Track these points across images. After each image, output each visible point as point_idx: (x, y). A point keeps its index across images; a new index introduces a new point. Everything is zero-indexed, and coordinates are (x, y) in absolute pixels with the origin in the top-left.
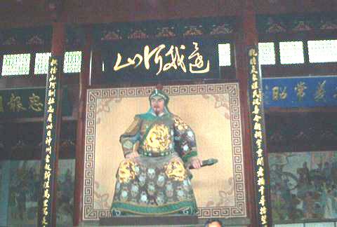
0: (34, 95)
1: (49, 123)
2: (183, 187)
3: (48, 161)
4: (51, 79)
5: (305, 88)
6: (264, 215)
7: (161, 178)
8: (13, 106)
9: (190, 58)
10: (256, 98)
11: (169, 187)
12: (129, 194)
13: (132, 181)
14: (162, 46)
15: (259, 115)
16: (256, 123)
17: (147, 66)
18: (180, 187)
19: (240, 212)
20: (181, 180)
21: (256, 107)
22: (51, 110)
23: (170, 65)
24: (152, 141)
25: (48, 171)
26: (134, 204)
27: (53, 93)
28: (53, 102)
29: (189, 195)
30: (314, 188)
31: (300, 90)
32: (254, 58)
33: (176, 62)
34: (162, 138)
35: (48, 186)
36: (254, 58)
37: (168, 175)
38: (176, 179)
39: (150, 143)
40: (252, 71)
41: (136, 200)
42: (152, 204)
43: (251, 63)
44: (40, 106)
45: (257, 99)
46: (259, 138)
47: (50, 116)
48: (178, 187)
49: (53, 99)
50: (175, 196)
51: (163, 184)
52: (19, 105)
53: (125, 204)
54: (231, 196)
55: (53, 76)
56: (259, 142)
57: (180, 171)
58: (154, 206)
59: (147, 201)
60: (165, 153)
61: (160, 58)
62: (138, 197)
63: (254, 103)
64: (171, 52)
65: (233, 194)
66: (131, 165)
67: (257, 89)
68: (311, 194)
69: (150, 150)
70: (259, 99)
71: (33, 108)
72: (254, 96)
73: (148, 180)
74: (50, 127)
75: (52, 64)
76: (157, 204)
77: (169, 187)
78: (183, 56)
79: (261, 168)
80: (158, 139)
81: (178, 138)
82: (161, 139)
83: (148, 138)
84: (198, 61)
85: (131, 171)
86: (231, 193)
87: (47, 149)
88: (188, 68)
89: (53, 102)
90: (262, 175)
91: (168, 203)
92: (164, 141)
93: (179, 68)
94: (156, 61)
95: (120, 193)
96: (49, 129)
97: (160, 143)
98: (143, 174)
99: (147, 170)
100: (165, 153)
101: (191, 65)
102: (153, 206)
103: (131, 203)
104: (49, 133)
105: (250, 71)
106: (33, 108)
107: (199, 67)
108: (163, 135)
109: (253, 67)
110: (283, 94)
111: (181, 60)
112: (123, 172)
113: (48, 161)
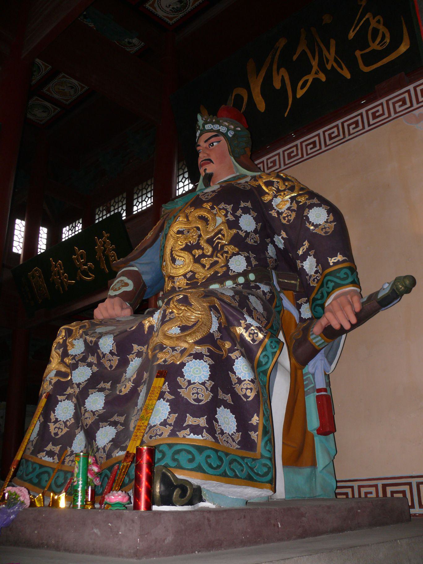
2: (174, 388)
9: (351, 35)
14: (282, 43)
17: (261, 106)
23: (310, 78)
33: (322, 66)
34: (203, 243)
41: (57, 449)
51: (130, 385)
61: (283, 72)
64: (302, 47)
78: (333, 42)
80: (188, 249)
82: (198, 246)
84: (375, 32)
88: (352, 66)
92: (209, 250)
93: (332, 74)
94: (277, 85)
97: (197, 260)
101: (358, 53)
107: (379, 48)
111: (331, 55)
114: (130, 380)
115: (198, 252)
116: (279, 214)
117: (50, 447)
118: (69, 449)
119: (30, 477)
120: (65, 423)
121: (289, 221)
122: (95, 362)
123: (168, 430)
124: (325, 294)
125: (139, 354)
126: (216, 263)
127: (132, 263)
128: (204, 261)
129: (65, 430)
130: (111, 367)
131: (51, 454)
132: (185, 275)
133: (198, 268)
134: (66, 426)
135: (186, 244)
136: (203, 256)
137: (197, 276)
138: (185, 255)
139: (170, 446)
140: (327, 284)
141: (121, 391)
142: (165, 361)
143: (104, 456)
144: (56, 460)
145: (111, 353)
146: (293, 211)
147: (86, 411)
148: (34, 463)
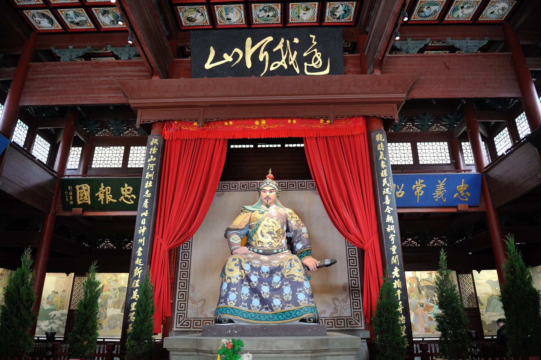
0: (126, 185)
1: (144, 210)
2: (304, 290)
3: (140, 254)
4: (149, 161)
5: (424, 186)
6: (402, 325)
7: (276, 279)
8: (101, 197)
10: (386, 186)
11: (287, 290)
12: (238, 297)
13: (242, 281)
15: (390, 205)
16: (388, 216)
18: (301, 289)
19: (357, 324)
20: (300, 280)
21: (387, 197)
22: (148, 194)
24: (263, 236)
25: (139, 266)
26: (244, 308)
27: (151, 175)
28: (150, 185)
29: (310, 300)
30: (426, 299)
31: (419, 187)
32: (382, 143)
35: (137, 285)
36: (382, 143)
37: (285, 275)
38: (296, 279)
39: (260, 238)
40: (381, 158)
41: (246, 304)
42: (267, 309)
43: (379, 149)
44: (132, 198)
45: (388, 189)
46: (392, 232)
47: (146, 201)
48: (298, 290)
49: (151, 182)
50: (295, 301)
51: (279, 285)
52: (109, 198)
53: (232, 308)
54: (346, 304)
55: (152, 156)
56: (392, 238)
57: (300, 270)
58: (269, 312)
59: (260, 306)
60: (278, 250)
62: (249, 301)
63: (384, 192)
65: (349, 302)
66: (240, 261)
67: (387, 177)
68: (422, 305)
69: (260, 245)
70: (390, 188)
71: (125, 201)
72: (384, 185)
73: (261, 281)
74: (146, 214)
75: (152, 144)
76: (273, 310)
77: (287, 290)
79: (396, 268)
80: (270, 233)
81: (290, 235)
83: (258, 232)
85: (242, 268)
86: (346, 302)
87: (140, 241)
89: (150, 185)
90: (398, 276)
91: (287, 309)
95: (227, 295)
96: (144, 217)
97: (273, 238)
98: (254, 272)
99: (260, 268)
100: (278, 250)
102: (267, 312)
103: (241, 307)
104: (143, 222)
105: (379, 158)
106: (125, 201)
108: (276, 229)
109: (381, 153)
110: (400, 192)
112: (231, 270)
113: (140, 254)
114: (278, 283)
115: (273, 236)
116: (292, 226)
117: (243, 304)
118: (251, 305)
119: (238, 314)
120: (246, 295)
121: (295, 229)
122: (258, 274)
123: (307, 302)
124: (302, 256)
125: (278, 275)
126: (278, 241)
127: (239, 230)
128: (275, 239)
129: (247, 298)
130: (265, 277)
131: (244, 306)
132: (268, 243)
133: (273, 241)
134: (247, 296)
135: (269, 231)
136: (275, 237)
137: (273, 244)
138: (269, 235)
139: (309, 306)
140: (304, 253)
141: (275, 287)
142: (297, 280)
143: (280, 308)
144: (247, 309)
145: (267, 273)
146: (297, 226)
147: (264, 293)
148: (238, 309)
